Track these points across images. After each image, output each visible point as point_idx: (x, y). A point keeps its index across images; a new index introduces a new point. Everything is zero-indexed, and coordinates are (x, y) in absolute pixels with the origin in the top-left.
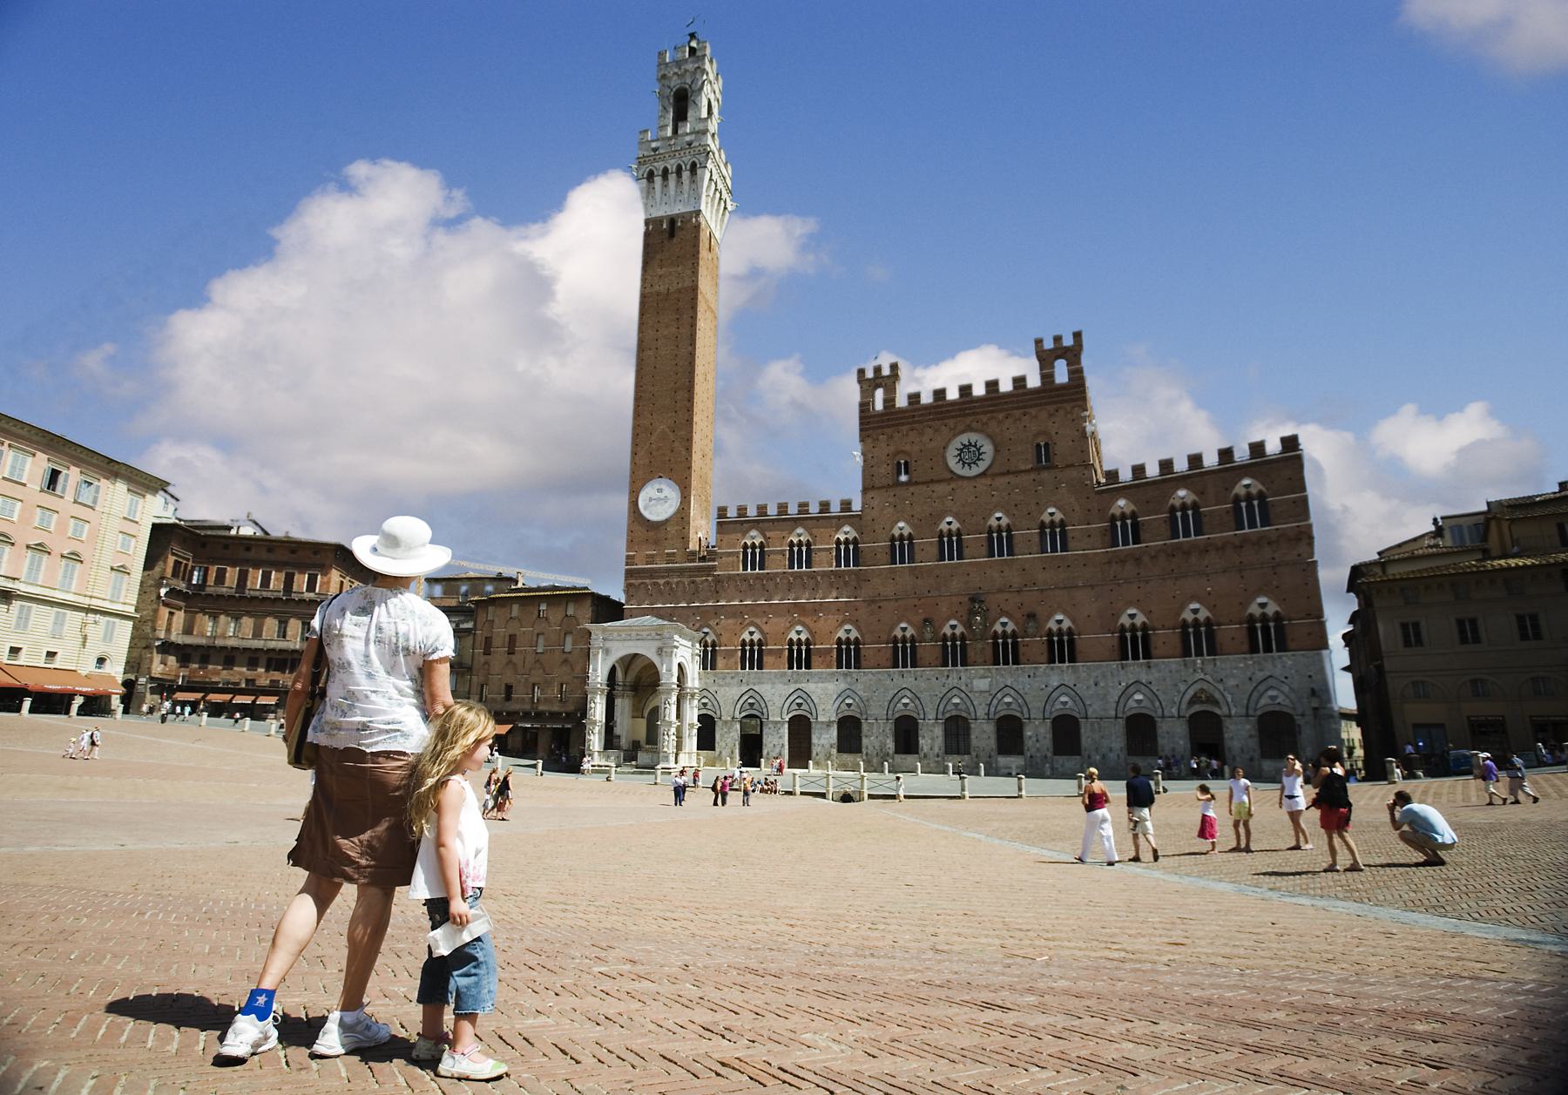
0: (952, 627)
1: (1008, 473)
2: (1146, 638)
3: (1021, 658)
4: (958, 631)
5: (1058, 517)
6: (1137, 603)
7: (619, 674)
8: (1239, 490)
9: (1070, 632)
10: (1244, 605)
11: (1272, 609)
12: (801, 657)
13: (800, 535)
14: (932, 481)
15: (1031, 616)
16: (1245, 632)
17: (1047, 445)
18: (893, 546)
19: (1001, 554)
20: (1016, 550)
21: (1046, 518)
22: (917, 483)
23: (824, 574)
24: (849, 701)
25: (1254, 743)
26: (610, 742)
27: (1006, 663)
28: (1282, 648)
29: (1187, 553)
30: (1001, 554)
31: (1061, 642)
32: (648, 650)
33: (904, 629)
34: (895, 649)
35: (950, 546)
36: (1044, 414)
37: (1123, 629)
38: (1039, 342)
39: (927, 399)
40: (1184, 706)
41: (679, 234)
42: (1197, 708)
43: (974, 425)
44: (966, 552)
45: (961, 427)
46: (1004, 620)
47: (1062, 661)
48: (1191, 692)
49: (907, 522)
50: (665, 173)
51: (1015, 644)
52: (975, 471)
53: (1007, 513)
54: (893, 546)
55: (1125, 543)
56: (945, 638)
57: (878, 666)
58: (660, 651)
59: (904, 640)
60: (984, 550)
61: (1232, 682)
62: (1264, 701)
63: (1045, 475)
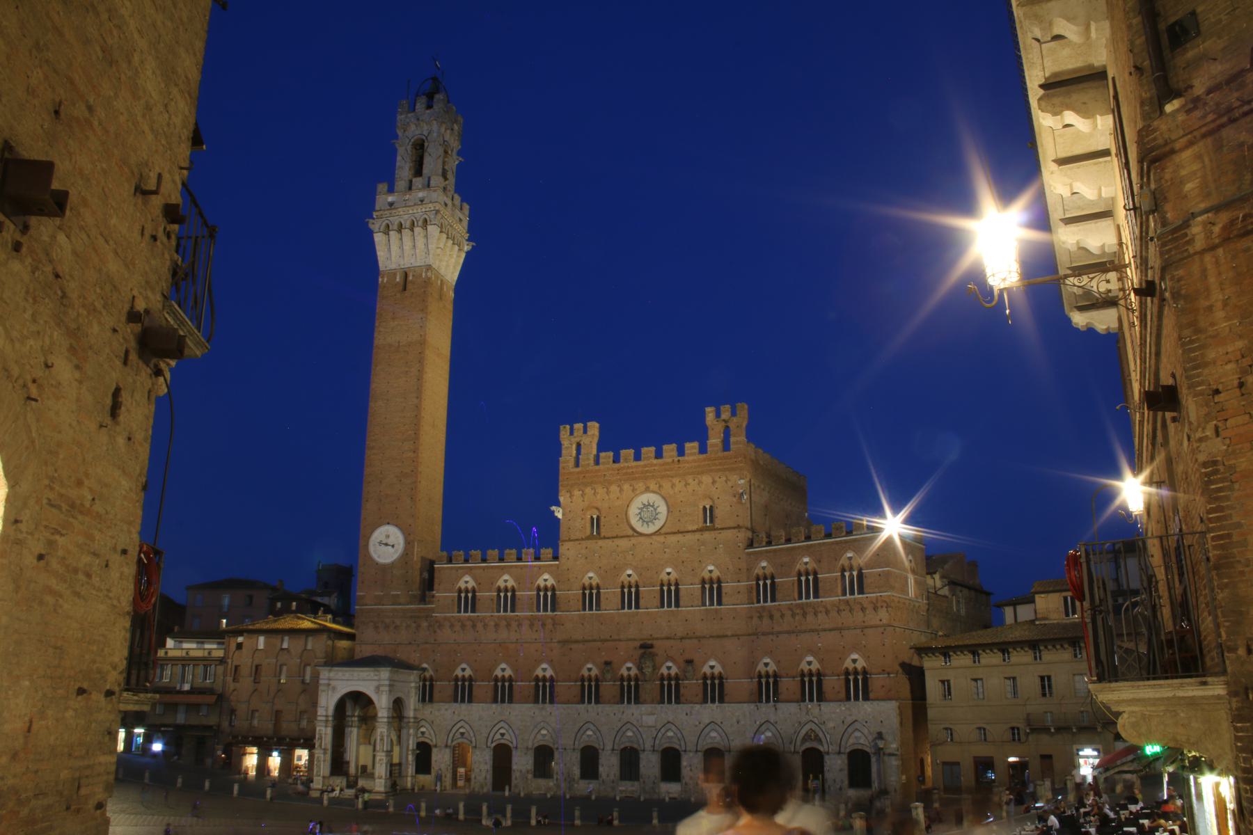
0: (628, 669)
1: (679, 532)
2: (776, 683)
3: (682, 699)
6: (770, 653)
8: (843, 561)
9: (721, 677)
10: (842, 660)
11: (861, 664)
12: (503, 692)
14: (617, 537)
16: (843, 683)
18: (584, 594)
19: (669, 605)
20: (681, 603)
21: (707, 576)
22: (605, 538)
23: (526, 618)
24: (544, 732)
25: (844, 777)
27: (670, 702)
28: (866, 698)
29: (804, 615)
30: (669, 605)
31: (713, 685)
33: (590, 670)
34: (583, 686)
35: (631, 596)
36: (710, 480)
37: (760, 676)
40: (798, 743)
41: (409, 286)
42: (808, 745)
43: (653, 486)
44: (642, 602)
45: (643, 489)
46: (669, 664)
47: (713, 701)
48: (803, 732)
49: (596, 573)
51: (677, 686)
53: (675, 567)
56: (622, 679)
57: (568, 702)
58: (378, 689)
59: (590, 680)
60: (657, 601)
61: (831, 725)
62: (851, 741)
63: (707, 536)
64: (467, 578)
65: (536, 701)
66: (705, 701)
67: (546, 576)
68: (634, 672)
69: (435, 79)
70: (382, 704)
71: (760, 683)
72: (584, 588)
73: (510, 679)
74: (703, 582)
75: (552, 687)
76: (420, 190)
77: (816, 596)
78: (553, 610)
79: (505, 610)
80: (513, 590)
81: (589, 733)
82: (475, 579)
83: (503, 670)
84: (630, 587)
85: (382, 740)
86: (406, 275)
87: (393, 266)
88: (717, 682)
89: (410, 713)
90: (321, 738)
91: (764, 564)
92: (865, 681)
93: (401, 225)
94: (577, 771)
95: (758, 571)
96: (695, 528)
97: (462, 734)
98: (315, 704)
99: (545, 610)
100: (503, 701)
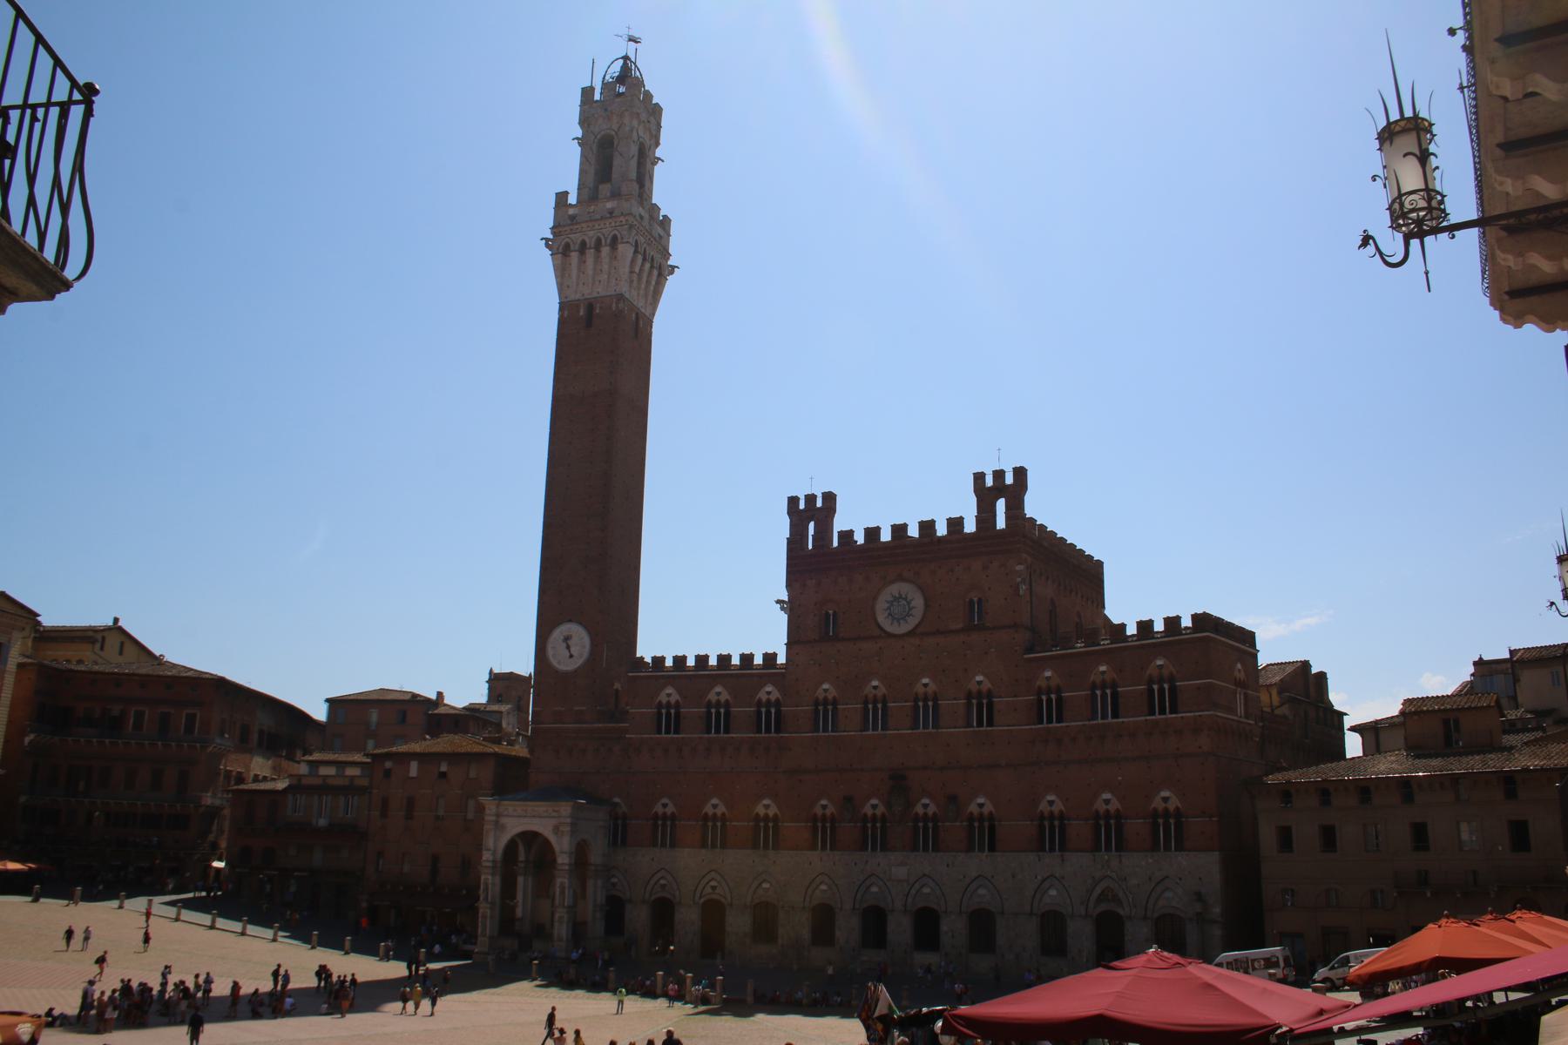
0: (873, 806)
4: (878, 812)
5: (987, 685)
7: (521, 849)
13: (719, 693)
15: (953, 799)
17: (980, 601)
18: (816, 712)
21: (974, 688)
24: (766, 885)
26: (507, 922)
27: (926, 849)
28: (1179, 848)
32: (544, 827)
33: (824, 807)
37: (1042, 817)
38: (979, 478)
39: (860, 538)
42: (1103, 907)
46: (926, 801)
47: (981, 849)
48: (1098, 890)
50: (583, 245)
51: (935, 828)
52: (904, 628)
54: (816, 712)
55: (1050, 721)
58: (556, 829)
59: (824, 818)
64: (669, 690)
65: (755, 846)
66: (969, 849)
67: (769, 688)
68: (881, 810)
69: (626, 58)
70: (563, 847)
71: (1041, 827)
72: (817, 703)
73: (723, 818)
74: (969, 696)
75: (776, 828)
76: (609, 199)
77: (1115, 716)
78: (778, 730)
79: (718, 731)
80: (727, 705)
81: (823, 887)
82: (679, 692)
83: (715, 806)
84: (875, 702)
85: (562, 892)
86: (590, 307)
87: (578, 296)
88: (986, 824)
89: (596, 857)
90: (486, 889)
91: (1048, 674)
92: (1178, 825)
93: (583, 244)
94: (806, 934)
95: (1041, 683)
96: (960, 626)
97: (663, 886)
98: (479, 847)
99: (768, 730)
100: (714, 846)
